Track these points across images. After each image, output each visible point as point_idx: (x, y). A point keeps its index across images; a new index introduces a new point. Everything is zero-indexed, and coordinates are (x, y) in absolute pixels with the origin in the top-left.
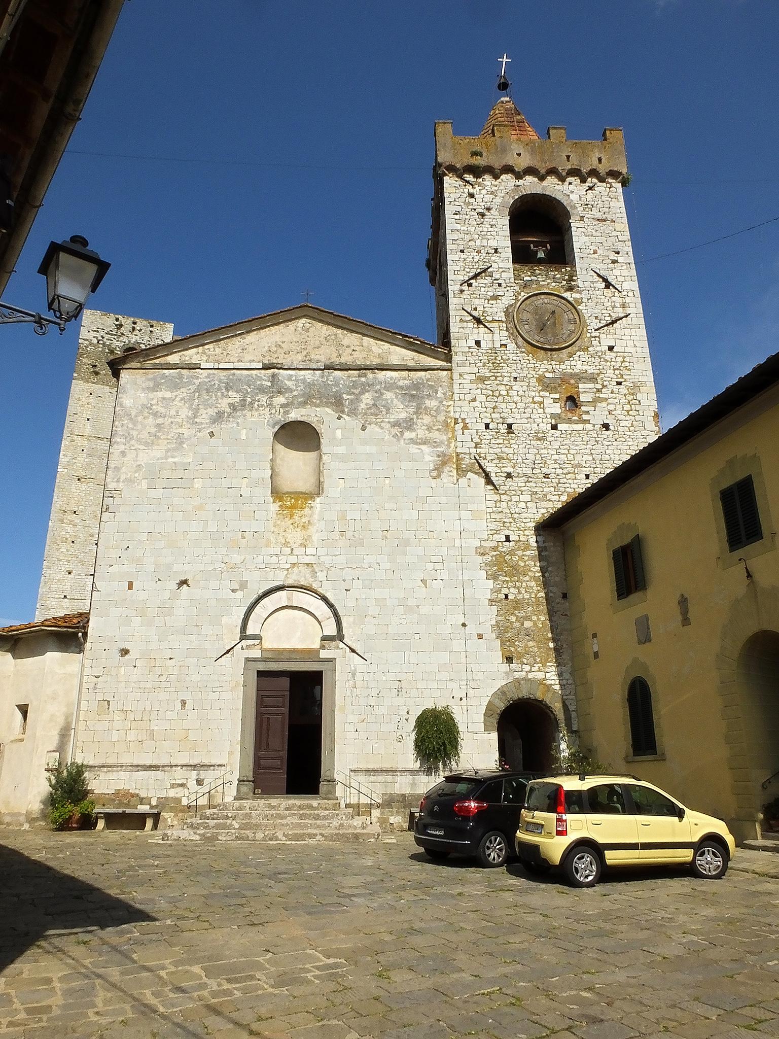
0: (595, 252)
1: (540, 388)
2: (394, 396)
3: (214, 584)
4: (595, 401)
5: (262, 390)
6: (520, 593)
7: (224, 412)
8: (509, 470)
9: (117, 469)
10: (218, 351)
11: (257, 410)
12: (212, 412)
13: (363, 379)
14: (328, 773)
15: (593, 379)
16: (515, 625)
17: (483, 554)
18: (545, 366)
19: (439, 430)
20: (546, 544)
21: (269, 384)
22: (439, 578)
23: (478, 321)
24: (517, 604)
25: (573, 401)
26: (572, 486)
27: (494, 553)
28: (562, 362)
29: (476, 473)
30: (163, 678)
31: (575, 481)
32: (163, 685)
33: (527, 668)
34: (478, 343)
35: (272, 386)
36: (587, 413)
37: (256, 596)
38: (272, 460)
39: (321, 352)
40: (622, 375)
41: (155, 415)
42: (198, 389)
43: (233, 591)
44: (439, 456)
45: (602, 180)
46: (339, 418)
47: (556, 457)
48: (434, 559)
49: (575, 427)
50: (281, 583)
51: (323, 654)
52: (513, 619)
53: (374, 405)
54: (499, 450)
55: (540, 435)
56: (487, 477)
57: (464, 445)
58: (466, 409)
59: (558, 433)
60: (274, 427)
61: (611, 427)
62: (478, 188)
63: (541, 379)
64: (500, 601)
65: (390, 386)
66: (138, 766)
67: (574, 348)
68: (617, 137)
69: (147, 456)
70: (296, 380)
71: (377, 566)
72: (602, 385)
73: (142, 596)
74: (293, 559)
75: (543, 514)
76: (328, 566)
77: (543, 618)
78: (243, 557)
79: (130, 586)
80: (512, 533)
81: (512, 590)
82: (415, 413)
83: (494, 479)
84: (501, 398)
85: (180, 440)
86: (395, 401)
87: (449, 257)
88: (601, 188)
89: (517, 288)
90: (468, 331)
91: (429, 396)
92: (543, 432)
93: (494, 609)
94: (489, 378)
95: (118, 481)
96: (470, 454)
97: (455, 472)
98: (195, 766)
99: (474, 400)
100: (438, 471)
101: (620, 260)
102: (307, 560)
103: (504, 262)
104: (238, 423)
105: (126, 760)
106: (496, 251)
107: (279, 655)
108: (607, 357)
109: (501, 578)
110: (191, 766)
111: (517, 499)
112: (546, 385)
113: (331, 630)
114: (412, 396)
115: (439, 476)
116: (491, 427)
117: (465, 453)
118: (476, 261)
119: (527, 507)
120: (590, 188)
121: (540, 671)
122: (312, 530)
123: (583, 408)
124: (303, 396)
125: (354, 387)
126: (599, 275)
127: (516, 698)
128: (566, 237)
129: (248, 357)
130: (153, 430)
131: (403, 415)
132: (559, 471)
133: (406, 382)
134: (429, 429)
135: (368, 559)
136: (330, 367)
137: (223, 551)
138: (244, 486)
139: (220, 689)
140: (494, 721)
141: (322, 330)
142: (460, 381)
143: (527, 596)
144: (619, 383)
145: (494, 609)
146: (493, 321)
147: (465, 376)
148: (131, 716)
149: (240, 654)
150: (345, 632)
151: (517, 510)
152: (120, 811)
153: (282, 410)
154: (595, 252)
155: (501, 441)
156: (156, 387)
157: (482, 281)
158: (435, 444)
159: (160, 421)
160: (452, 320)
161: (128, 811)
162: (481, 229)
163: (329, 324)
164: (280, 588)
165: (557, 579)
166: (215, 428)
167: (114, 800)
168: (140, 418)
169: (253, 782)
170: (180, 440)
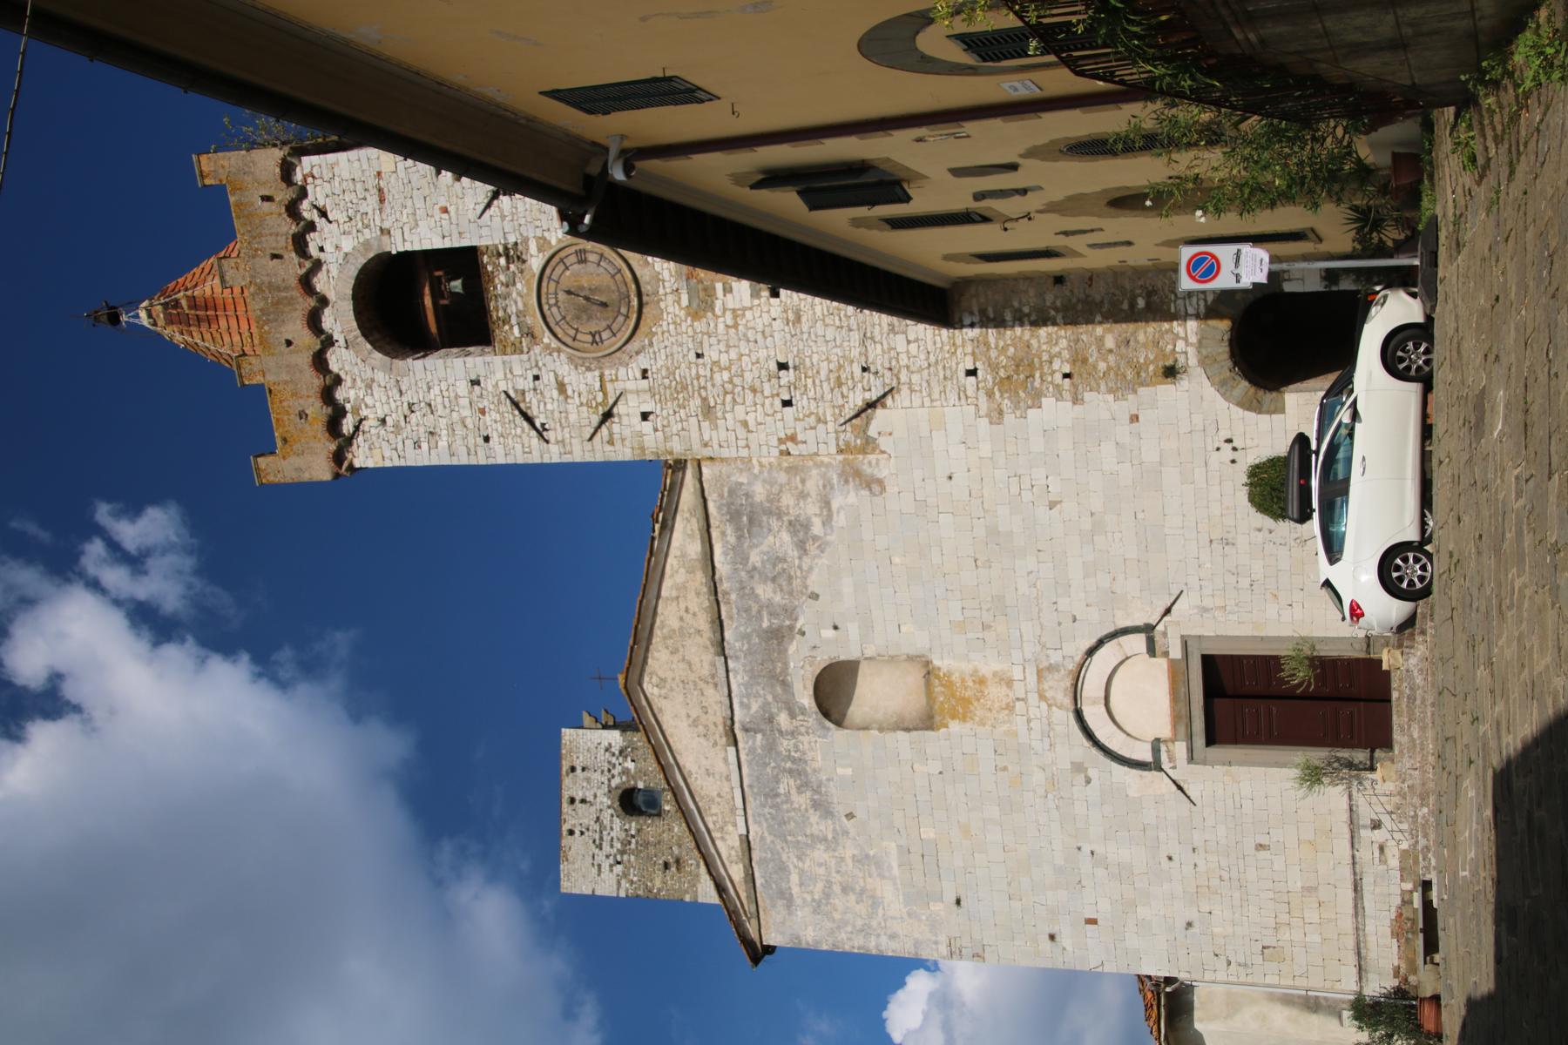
0: (445, 210)
1: (709, 314)
5: (771, 747)
6: (1059, 354)
7: (813, 800)
9: (917, 944)
10: (714, 810)
12: (814, 817)
13: (733, 597)
14: (1357, 646)
16: (1112, 364)
17: (1001, 413)
20: (975, 309)
21: (759, 736)
23: (608, 415)
24: (1079, 359)
29: (868, 424)
30: (1226, 876)
32: (1234, 874)
33: (1180, 346)
35: (760, 731)
37: (1095, 751)
38: (881, 730)
43: (1088, 781)
44: (847, 482)
45: (303, 193)
46: (803, 634)
48: (1014, 490)
51: (1176, 653)
52: (1102, 366)
53: (774, 580)
54: (825, 385)
55: (791, 316)
56: (871, 405)
57: (823, 442)
58: (763, 436)
60: (829, 729)
64: (1075, 387)
65: (739, 556)
66: (1356, 906)
68: (214, 166)
70: (748, 696)
74: (1033, 698)
76: (1038, 648)
79: (1092, 921)
81: (1056, 365)
82: (779, 517)
85: (862, 860)
86: (764, 548)
87: (501, 460)
88: (317, 194)
89: (537, 349)
90: (627, 433)
91: (747, 495)
92: (785, 311)
93: (1087, 396)
94: (705, 400)
95: (936, 943)
97: (871, 457)
98: (1352, 831)
99: (745, 424)
100: (873, 484)
102: (1032, 678)
103: (493, 369)
105: (1347, 923)
107: (1180, 717)
109: (1037, 384)
111: (903, 357)
113: (1137, 642)
114: (751, 521)
115: (880, 482)
116: (787, 398)
117: (837, 439)
118: (500, 419)
119: (917, 340)
124: (772, 686)
125: (747, 610)
126: (488, 206)
127: (1229, 364)
129: (720, 767)
130: (852, 898)
131: (786, 537)
133: (729, 532)
134: (803, 496)
136: (721, 646)
139: (1237, 798)
140: (1268, 397)
141: (660, 660)
142: (716, 446)
143: (1064, 343)
145: (1087, 396)
146: (602, 388)
147: (706, 438)
148: (1284, 918)
149: (1182, 770)
150: (1140, 623)
151: (923, 357)
152: (1421, 936)
154: (445, 210)
155: (809, 381)
158: (828, 485)
159: (837, 889)
160: (613, 458)
162: (440, 407)
163: (647, 650)
164: (1079, 715)
165: (1032, 292)
166: (841, 810)
168: (837, 916)
169: (1372, 752)
170: (862, 860)
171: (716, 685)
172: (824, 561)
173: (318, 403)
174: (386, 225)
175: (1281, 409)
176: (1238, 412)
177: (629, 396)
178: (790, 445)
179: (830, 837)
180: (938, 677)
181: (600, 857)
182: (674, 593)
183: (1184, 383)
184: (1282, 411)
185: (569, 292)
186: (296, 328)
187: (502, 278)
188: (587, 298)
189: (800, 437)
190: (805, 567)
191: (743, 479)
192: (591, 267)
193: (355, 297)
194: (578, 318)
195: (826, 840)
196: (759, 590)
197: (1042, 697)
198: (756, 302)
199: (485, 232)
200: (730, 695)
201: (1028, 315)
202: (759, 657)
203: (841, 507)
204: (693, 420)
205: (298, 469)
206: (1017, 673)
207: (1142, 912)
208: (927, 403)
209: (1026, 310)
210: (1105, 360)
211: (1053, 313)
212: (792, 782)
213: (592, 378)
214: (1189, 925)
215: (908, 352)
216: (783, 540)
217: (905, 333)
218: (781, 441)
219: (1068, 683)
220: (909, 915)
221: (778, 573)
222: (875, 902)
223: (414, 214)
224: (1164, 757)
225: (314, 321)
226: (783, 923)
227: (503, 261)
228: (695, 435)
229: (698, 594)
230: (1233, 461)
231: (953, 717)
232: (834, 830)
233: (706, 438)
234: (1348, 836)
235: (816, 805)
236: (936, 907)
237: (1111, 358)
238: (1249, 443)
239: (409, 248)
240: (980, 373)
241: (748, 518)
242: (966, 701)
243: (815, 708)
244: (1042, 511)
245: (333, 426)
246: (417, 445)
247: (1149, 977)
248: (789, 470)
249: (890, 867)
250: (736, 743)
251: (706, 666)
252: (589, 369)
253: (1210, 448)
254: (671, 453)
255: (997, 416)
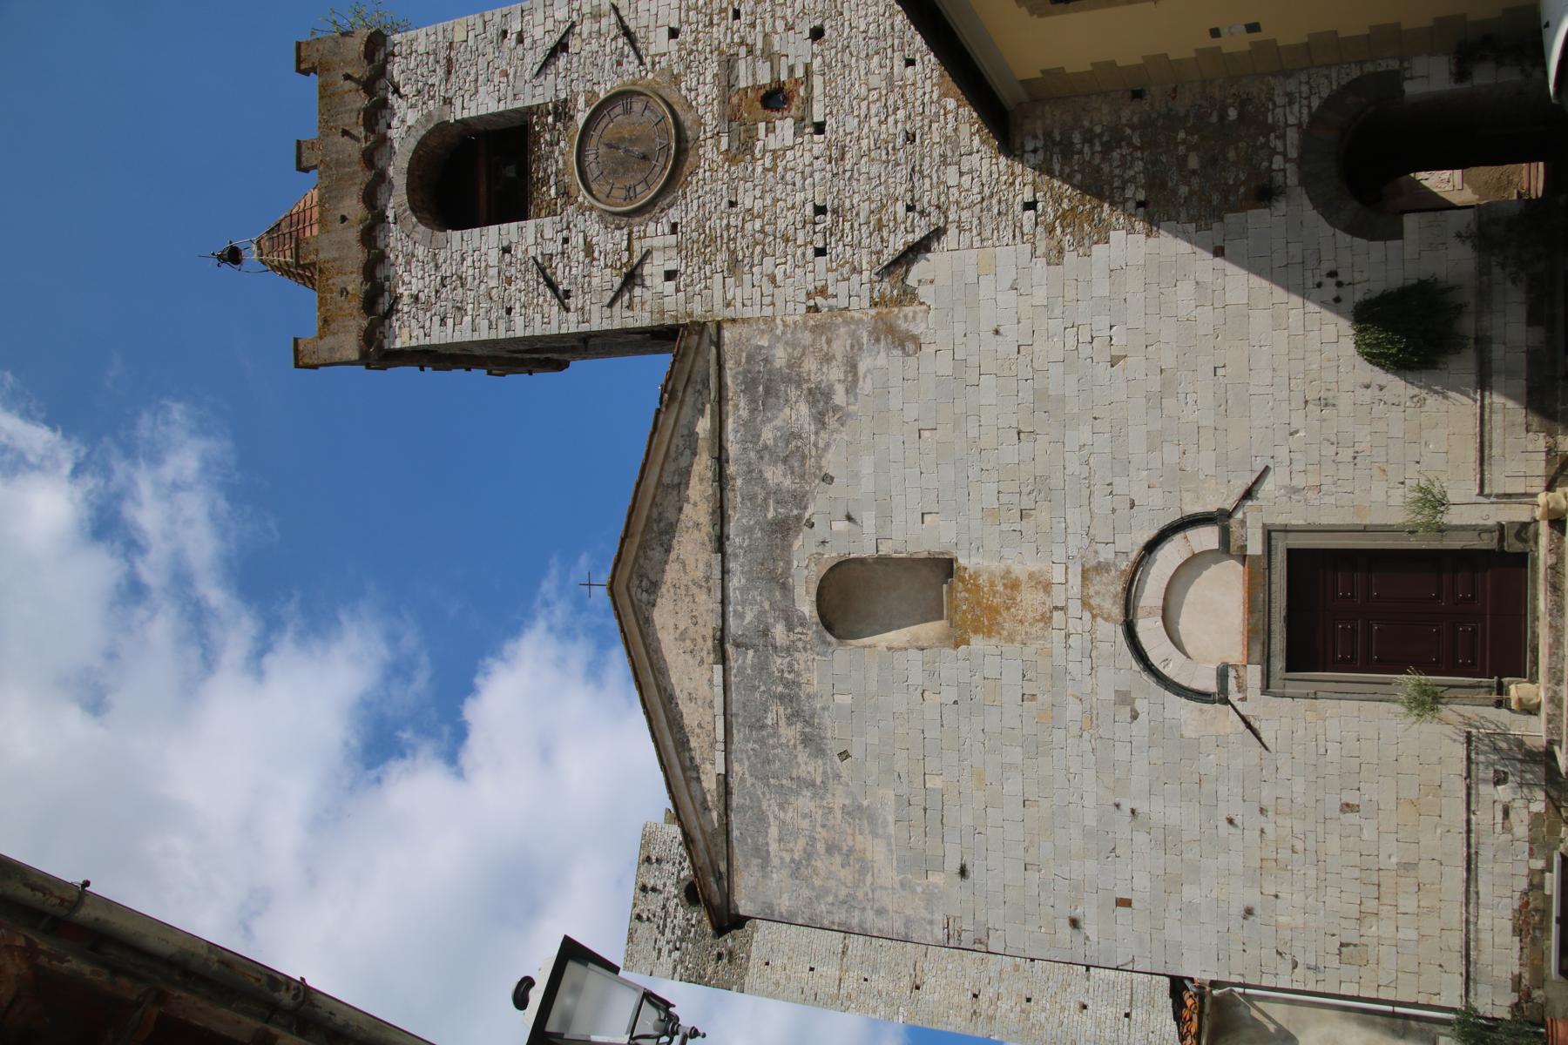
2: (769, 426)
3: (1121, 753)
4: (770, 56)
5: (762, 667)
6: (1133, 179)
7: (803, 733)
8: (900, 208)
9: (908, 922)
11: (798, 674)
12: (802, 756)
13: (739, 482)
15: (729, 64)
17: (1061, 251)
18: (709, 153)
19: (829, 342)
20: (1040, 133)
21: (751, 653)
22: (1107, 332)
25: (774, 98)
26: (928, 89)
27: (1059, 230)
28: (700, 122)
30: (1299, 846)
31: (919, 84)
33: (1278, 162)
34: (670, 275)
36: (791, 69)
37: (1145, 677)
39: (692, 559)
40: (722, 10)
41: (809, 855)
42: (764, 780)
43: (1135, 716)
44: (878, 340)
47: (874, 121)
48: (1071, 344)
49: (818, 90)
50: (1120, 630)
51: (1255, 547)
52: (1184, 190)
53: (785, 460)
54: (864, 228)
55: (835, 153)
57: (855, 294)
59: (831, 122)
60: (829, 644)
61: (818, 23)
62: (401, 290)
63: (731, 158)
65: (751, 432)
67: (673, 98)
69: (886, 871)
70: (743, 603)
71: (1085, 452)
72: (742, 43)
73: (1142, 881)
74: (1075, 608)
75: (983, 142)
76: (1086, 541)
77: (1182, 135)
78: (1071, 699)
79: (1124, 903)
80: (1019, 198)
81: (1129, 194)
82: (799, 386)
83: (918, 235)
84: (768, 229)
85: (854, 812)
86: (778, 422)
87: (519, 333)
88: (396, 70)
89: (570, 209)
91: (766, 360)
95: (931, 922)
96: (870, 281)
97: (909, 310)
98: (1469, 788)
99: (773, 279)
100: (905, 342)
101: (516, 27)
102: (1075, 580)
103: (526, 235)
104: (823, 709)
105: (1455, 914)
106: (506, 250)
107: (1257, 634)
108: (690, 39)
110: (1469, 795)
112: (742, 149)
114: (767, 391)
116: (820, 245)
117: (872, 290)
119: (971, 172)
120: (396, 91)
121: (1283, 137)
122: (1019, 572)
123: (784, 77)
125: (752, 498)
126: (545, 65)
128: (481, 128)
129: (704, 690)
130: (838, 859)
131: (803, 408)
132: (901, 114)
133: (742, 404)
134: (827, 359)
135: (1074, 467)
137: (1059, 735)
138: (938, 698)
139: (1321, 742)
142: (739, 305)
143: (1139, 165)
144: (737, 15)
146: (629, 248)
147: (729, 296)
148: (1371, 905)
149: (1256, 704)
150: (1210, 505)
151: (976, 190)
153: (799, 629)
155: (847, 225)
156: (762, 854)
157: (559, 273)
158: (857, 345)
159: (821, 847)
160: (631, 324)
161: (1555, 911)
166: (834, 747)
167: (1534, 939)
168: (817, 882)
170: (854, 812)
171: (709, 590)
172: (843, 436)
173: (360, 279)
174: (450, 94)
175: (1399, 235)
176: (1344, 238)
177: (655, 254)
178: (819, 300)
179: (818, 781)
180: (963, 580)
181: (662, 943)
182: (676, 480)
183: (1281, 206)
184: (1399, 235)
185: (610, 146)
186: (353, 206)
187: (548, 137)
188: (626, 151)
189: (830, 290)
190: (821, 445)
191: (764, 342)
192: (634, 118)
193: (410, 171)
194: (615, 171)
195: (813, 785)
196: (768, 475)
197: (1086, 604)
198: (799, 140)
199: (540, 90)
200: (724, 602)
201: (1100, 136)
202: (760, 555)
203: (868, 371)
204: (718, 277)
205: (331, 350)
206: (1057, 575)
207: (1190, 892)
208: (977, 244)
209: (1098, 129)
210: (1188, 184)
211: (1128, 131)
212: (781, 710)
213: (620, 236)
214: (1249, 912)
215: (959, 186)
216: (798, 413)
217: (958, 163)
218: (809, 295)
219: (1119, 587)
220: (902, 885)
221: (792, 452)
222: (864, 868)
223: (476, 80)
224: (1232, 685)
225: (371, 197)
226: (755, 888)
227: (550, 119)
228: (718, 294)
229: (701, 480)
230: (1337, 300)
231: (975, 632)
232: (825, 773)
233: (729, 296)
234: (1463, 794)
235: (806, 740)
236: (936, 878)
237: (1195, 181)
238: (1358, 277)
239: (466, 114)
240: (1040, 206)
241: (767, 387)
242: (993, 611)
243: (816, 618)
244: (1103, 369)
245: (370, 302)
246: (443, 322)
247: (1192, 980)
248: (814, 329)
249: (885, 824)
250: (723, 659)
251: (701, 566)
252: (619, 228)
253: (1310, 284)
254: (690, 315)
255: (1056, 256)
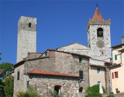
18: (99, 49)
25: (103, 53)
63: (100, 51)
103: (96, 37)
112: (100, 51)
